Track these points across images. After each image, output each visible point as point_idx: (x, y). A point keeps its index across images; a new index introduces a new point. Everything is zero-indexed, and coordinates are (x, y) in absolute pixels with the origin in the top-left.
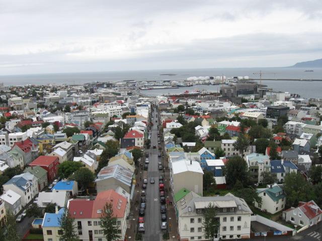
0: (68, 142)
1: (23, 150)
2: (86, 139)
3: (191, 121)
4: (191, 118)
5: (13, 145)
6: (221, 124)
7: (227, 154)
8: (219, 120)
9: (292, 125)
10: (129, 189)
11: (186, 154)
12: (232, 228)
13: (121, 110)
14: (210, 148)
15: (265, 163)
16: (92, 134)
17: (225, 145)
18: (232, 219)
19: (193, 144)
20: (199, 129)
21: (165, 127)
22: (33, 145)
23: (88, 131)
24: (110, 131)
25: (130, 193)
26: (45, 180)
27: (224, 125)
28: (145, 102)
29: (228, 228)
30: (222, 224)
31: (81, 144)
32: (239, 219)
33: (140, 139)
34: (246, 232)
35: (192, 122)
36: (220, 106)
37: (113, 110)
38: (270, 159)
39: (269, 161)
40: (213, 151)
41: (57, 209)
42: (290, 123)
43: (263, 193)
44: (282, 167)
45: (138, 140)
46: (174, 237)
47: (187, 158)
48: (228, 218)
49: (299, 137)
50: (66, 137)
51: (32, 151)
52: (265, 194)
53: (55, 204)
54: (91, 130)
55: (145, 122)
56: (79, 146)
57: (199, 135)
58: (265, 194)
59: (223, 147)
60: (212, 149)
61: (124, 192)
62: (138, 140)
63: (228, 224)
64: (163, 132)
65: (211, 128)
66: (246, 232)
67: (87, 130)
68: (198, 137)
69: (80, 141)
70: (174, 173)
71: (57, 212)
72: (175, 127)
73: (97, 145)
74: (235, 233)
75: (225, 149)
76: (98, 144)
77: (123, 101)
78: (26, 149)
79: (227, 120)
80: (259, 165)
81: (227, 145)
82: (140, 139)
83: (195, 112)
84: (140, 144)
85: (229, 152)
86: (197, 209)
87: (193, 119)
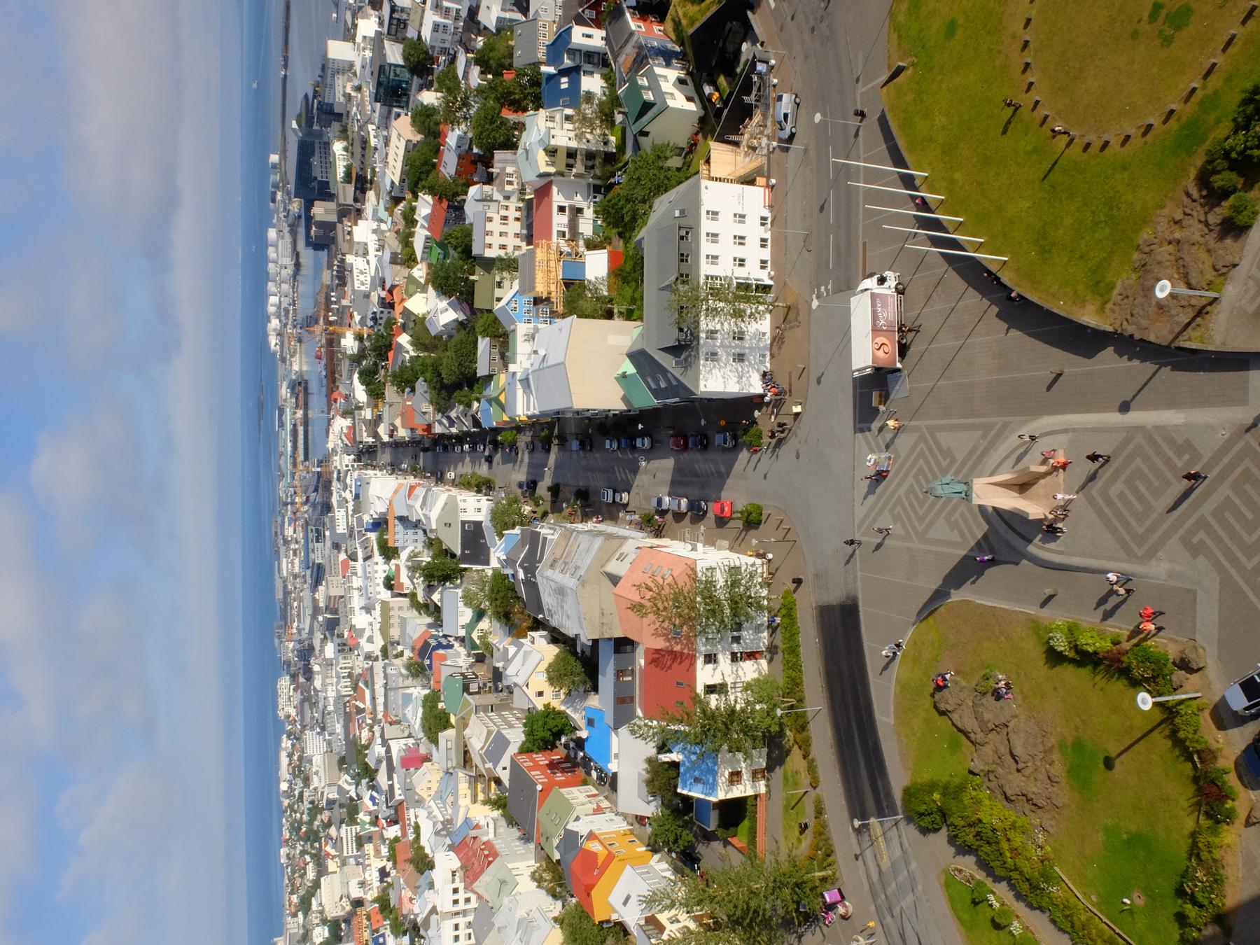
0: (465, 726)
1: (490, 863)
2: (459, 670)
3: (409, 348)
5: (473, 897)
6: (423, 252)
8: (410, 260)
9: (436, 27)
10: (617, 542)
12: (740, 240)
15: (550, 124)
16: (441, 651)
18: (714, 237)
19: (483, 344)
22: (473, 833)
23: (436, 663)
24: (436, 597)
25: (625, 538)
26: (579, 796)
29: (740, 252)
30: (724, 269)
31: (474, 687)
32: (714, 214)
34: (755, 199)
35: (417, 343)
36: (366, 254)
38: (537, 109)
39: (542, 113)
40: (506, 283)
41: (665, 758)
42: (427, 33)
43: (642, 139)
44: (564, 73)
48: (706, 248)
49: (473, 12)
50: (450, 733)
51: (491, 836)
52: (646, 134)
53: (650, 761)
54: (430, 658)
55: (412, 488)
56: (478, 693)
58: (646, 134)
60: (499, 285)
61: (622, 558)
63: (726, 250)
66: (755, 199)
67: (430, 666)
69: (466, 688)
71: (675, 756)
73: (479, 637)
74: (755, 231)
75: (503, 247)
76: (475, 635)
78: (486, 856)
79: (412, 234)
80: (553, 142)
81: (488, 239)
83: (381, 328)
84: (478, 505)
85: (511, 235)
87: (404, 339)
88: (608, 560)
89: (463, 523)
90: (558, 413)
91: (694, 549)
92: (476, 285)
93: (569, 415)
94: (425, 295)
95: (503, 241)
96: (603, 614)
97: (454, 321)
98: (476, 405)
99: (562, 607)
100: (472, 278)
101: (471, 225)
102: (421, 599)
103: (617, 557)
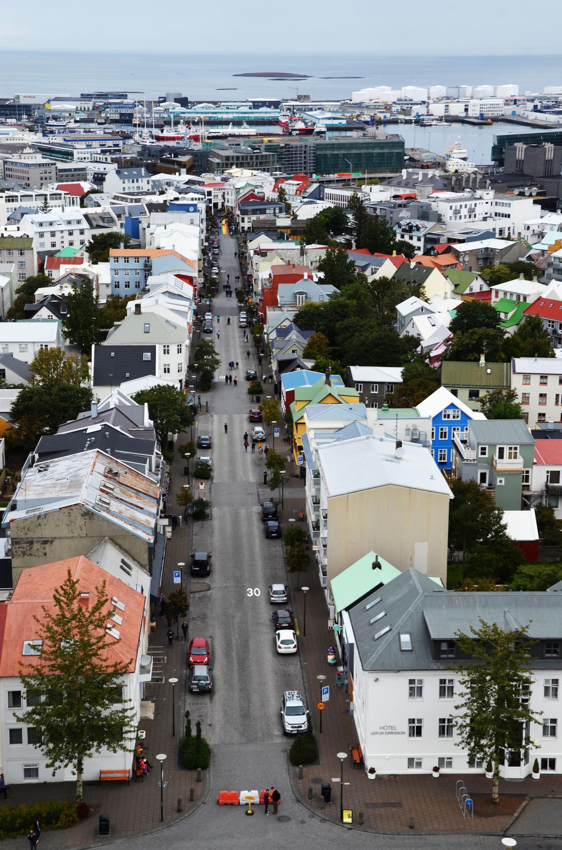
3: (377, 277)
4: (381, 265)
6: (505, 293)
7: (533, 418)
11: (373, 413)
13: (85, 225)
14: (464, 393)
17: (527, 376)
20: (415, 313)
21: (274, 303)
24: (45, 312)
27: (518, 296)
28: (185, 192)
33: (173, 349)
37: (51, 224)
45: (166, 351)
46: (342, 755)
47: (378, 432)
55: (189, 280)
57: (413, 333)
59: (516, 383)
60: (474, 394)
61: (125, 567)
62: (166, 351)
64: (264, 320)
65: (459, 309)
68: (415, 341)
70: (333, 492)
72: (316, 300)
75: (526, 398)
77: (86, 186)
79: (529, 277)
81: (535, 380)
82: (173, 349)
84: (174, 369)
85: (542, 409)
86: (438, 642)
88: (121, 548)
89: (152, 349)
90: (317, 475)
91: (143, 669)
92: (474, 364)
93: (310, 490)
94: (449, 294)
95: (534, 399)
96: (45, 542)
97: (419, 335)
98: (310, 364)
99: (54, 486)
100: (483, 358)
101: (553, 356)
102: (41, 292)
103: (126, 560)
